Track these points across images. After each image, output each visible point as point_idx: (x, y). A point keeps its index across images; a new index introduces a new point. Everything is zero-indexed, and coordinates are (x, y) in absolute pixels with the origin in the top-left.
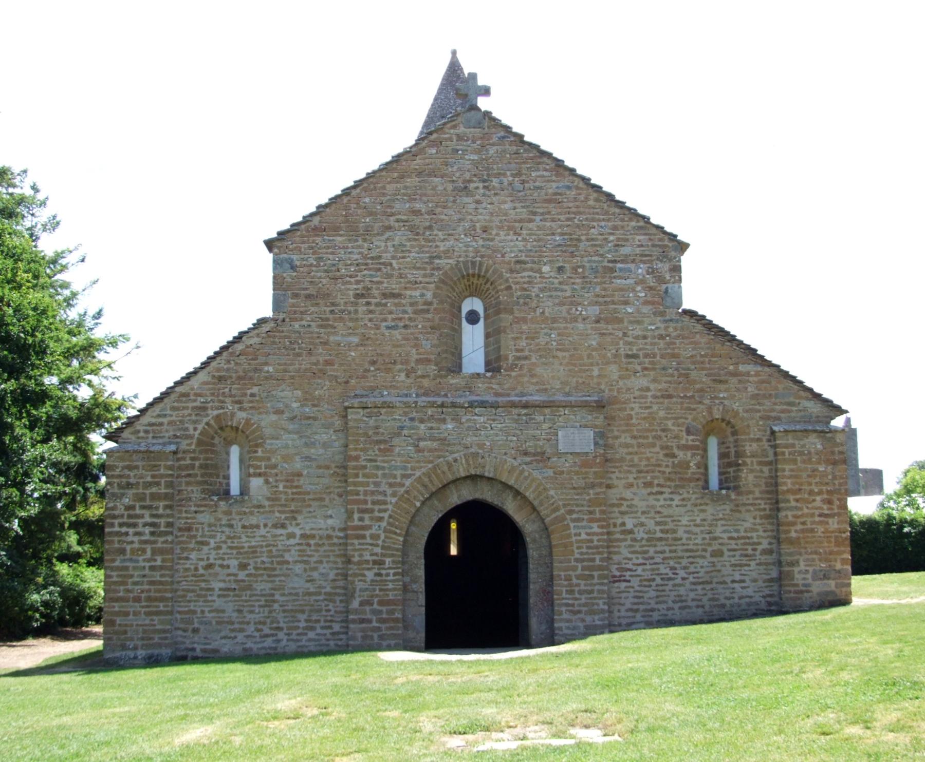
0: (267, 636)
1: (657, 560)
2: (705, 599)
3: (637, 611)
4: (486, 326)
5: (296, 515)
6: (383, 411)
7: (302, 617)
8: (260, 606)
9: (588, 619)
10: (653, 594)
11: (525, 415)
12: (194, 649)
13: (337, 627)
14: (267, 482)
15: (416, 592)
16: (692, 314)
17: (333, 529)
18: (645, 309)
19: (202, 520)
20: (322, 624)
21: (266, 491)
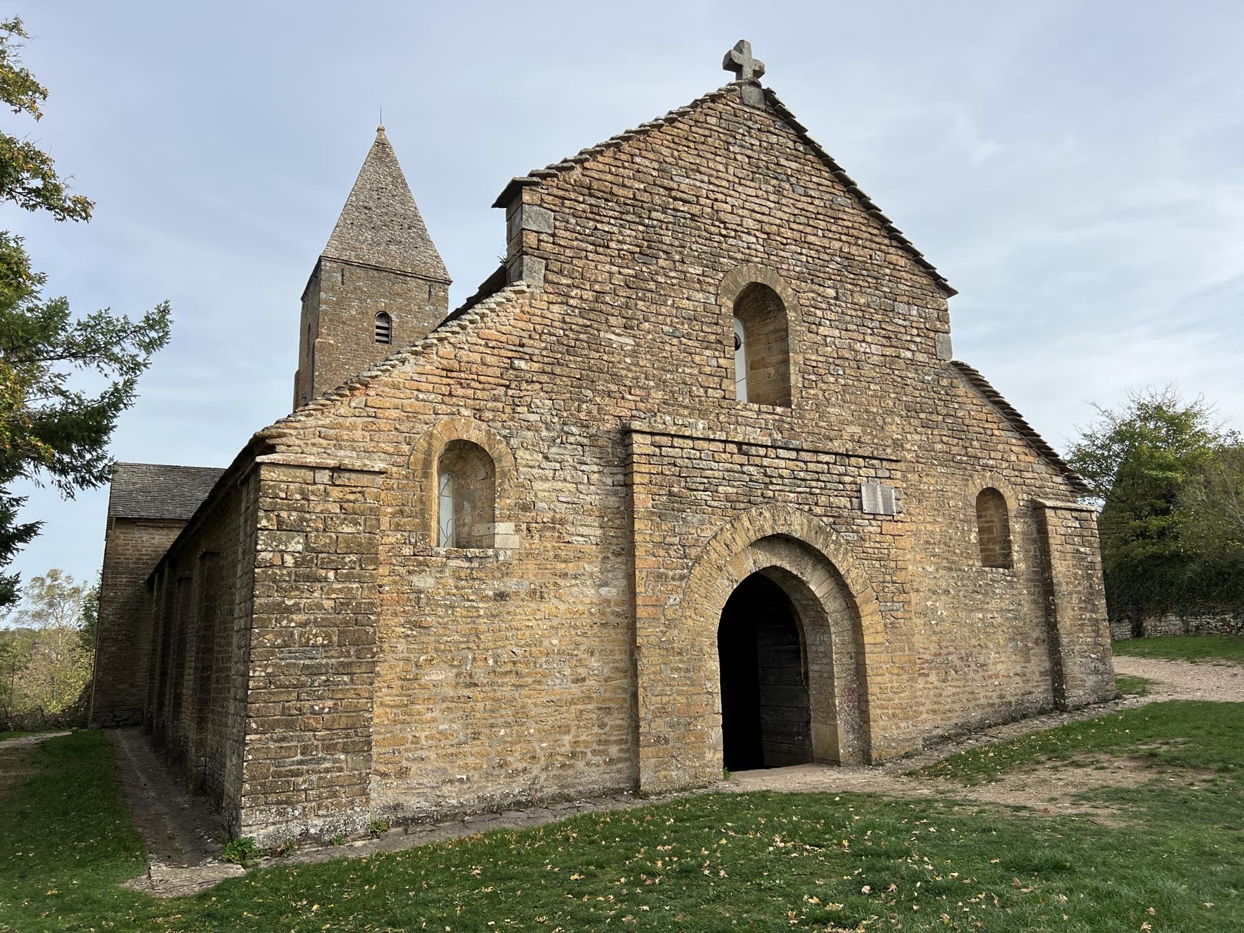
0: (516, 772)
1: (951, 649)
2: (995, 695)
3: (934, 712)
4: (748, 354)
5: (561, 582)
6: (677, 442)
7: (567, 739)
8: (508, 725)
9: (903, 725)
10: (950, 690)
11: (827, 463)
12: (397, 807)
13: (614, 751)
14: (518, 530)
15: (711, 693)
16: (962, 369)
17: (608, 602)
18: (921, 357)
19: (422, 585)
20: (595, 746)
21: (515, 541)
